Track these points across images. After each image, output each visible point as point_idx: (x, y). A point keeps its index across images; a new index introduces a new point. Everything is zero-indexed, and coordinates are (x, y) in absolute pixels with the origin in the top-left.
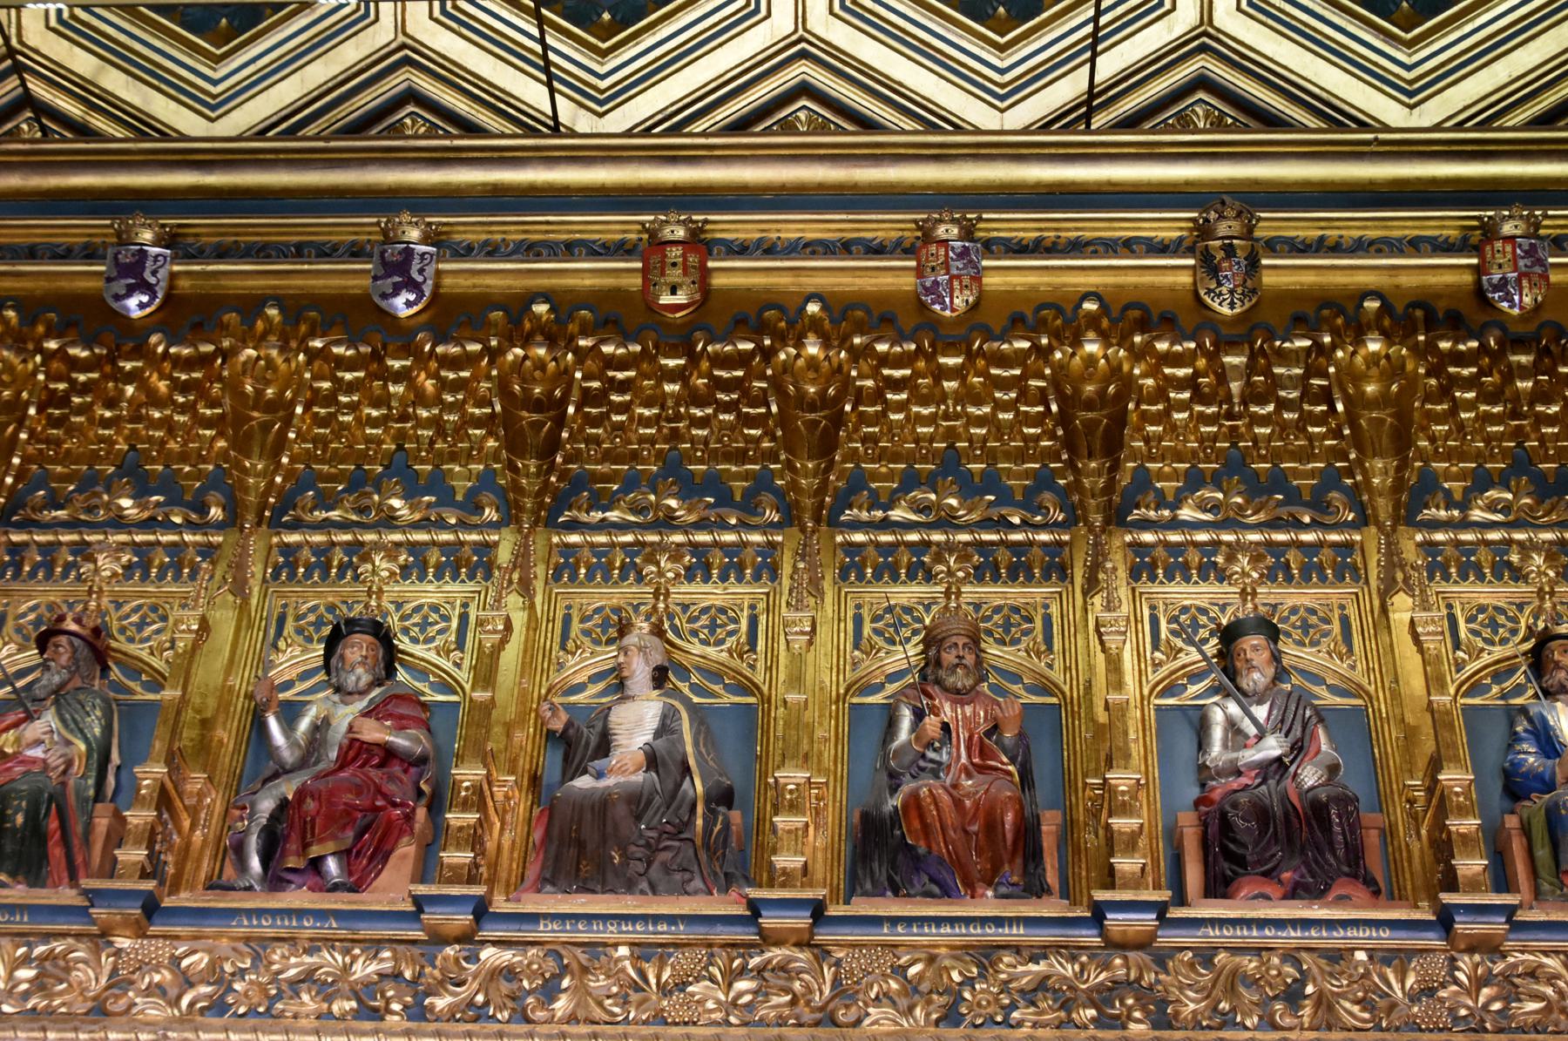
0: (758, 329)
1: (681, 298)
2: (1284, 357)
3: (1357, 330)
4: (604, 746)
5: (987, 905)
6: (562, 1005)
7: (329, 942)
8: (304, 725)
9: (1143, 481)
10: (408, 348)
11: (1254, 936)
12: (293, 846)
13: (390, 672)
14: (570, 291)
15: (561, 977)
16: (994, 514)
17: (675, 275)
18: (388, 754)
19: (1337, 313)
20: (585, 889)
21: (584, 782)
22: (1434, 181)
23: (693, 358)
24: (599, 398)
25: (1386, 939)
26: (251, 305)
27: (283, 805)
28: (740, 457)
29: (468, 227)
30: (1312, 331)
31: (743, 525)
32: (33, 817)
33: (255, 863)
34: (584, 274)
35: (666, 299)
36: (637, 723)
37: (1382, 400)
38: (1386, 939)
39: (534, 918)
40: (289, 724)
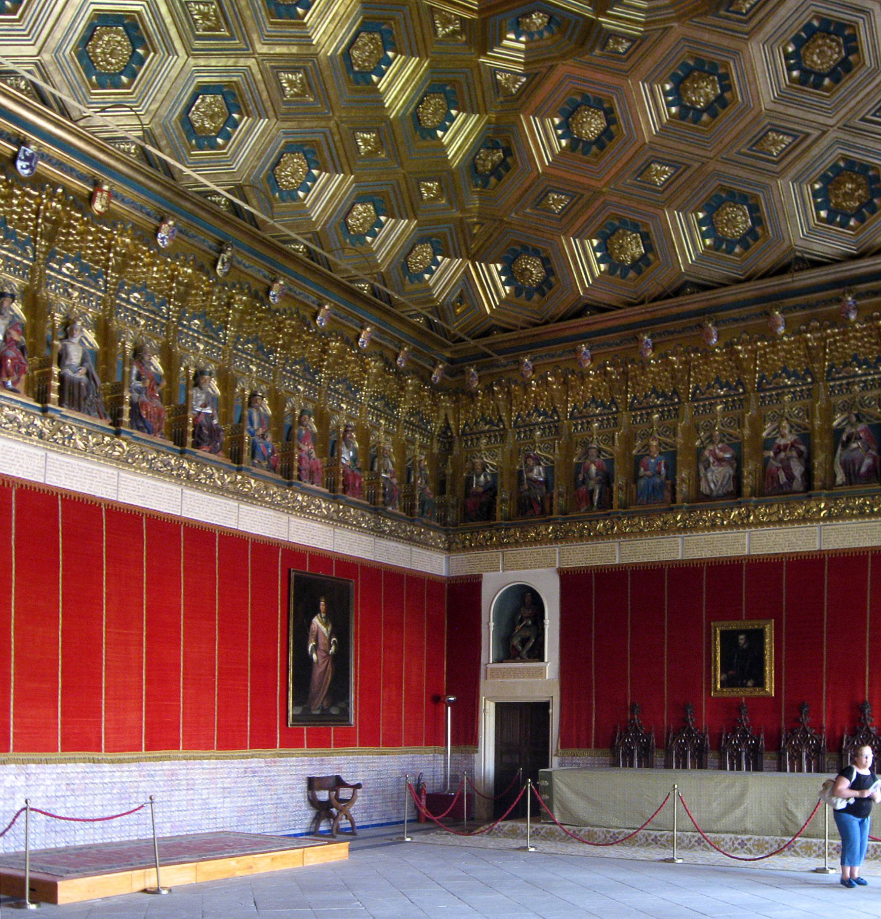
36: (75, 355)
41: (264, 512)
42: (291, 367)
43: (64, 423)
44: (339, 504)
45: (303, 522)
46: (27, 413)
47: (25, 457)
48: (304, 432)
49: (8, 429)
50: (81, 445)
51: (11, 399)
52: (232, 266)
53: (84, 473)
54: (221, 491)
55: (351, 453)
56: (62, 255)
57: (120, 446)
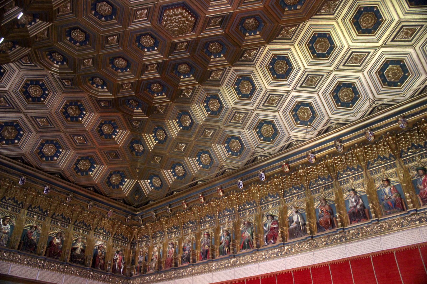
0: (296, 170)
2: (349, 154)
3: (355, 148)
4: (293, 221)
5: (328, 231)
6: (293, 251)
8: (267, 226)
9: (339, 173)
11: (354, 228)
13: (273, 218)
19: (353, 147)
21: (291, 227)
22: (360, 126)
23: (291, 176)
24: (284, 182)
25: (367, 225)
27: (267, 236)
28: (299, 184)
30: (351, 150)
31: (301, 191)
32: (248, 243)
34: (277, 170)
37: (361, 155)
38: (367, 225)
40: (266, 227)
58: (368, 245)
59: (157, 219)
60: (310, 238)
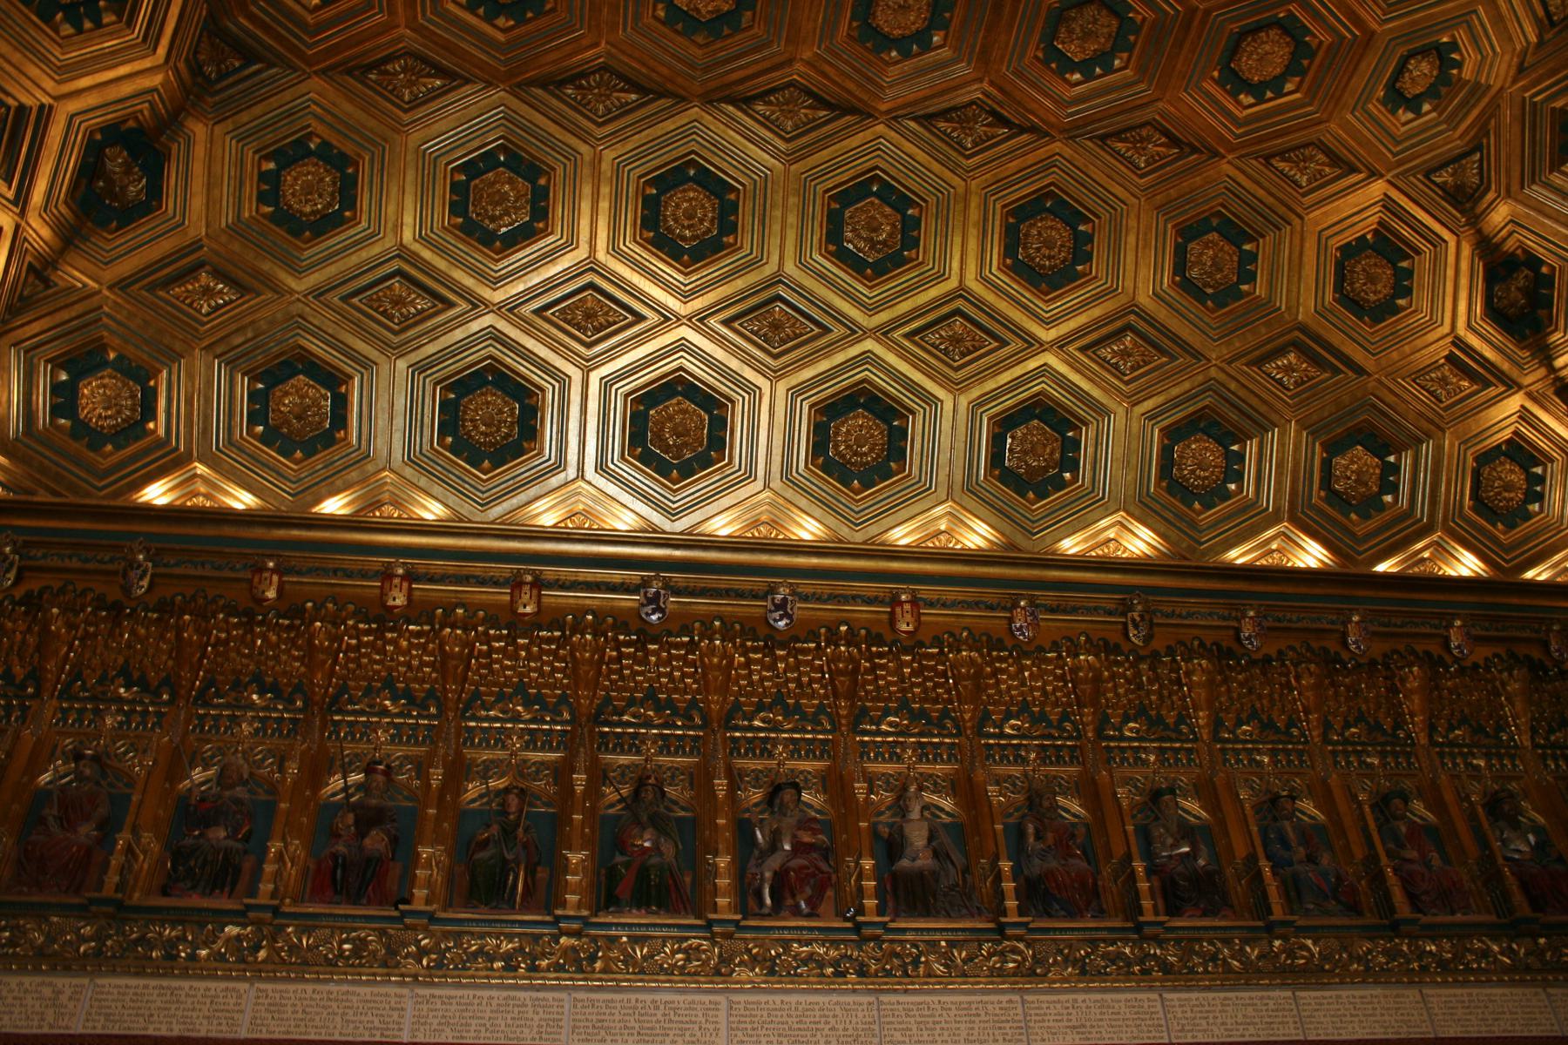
1: (911, 628)
7: (816, 940)
10: (783, 646)
12: (787, 895)
14: (857, 620)
15: (919, 957)
16: (1046, 732)
17: (908, 617)
18: (811, 847)
20: (921, 915)
21: (905, 863)
26: (706, 621)
27: (775, 873)
29: (807, 585)
33: (768, 901)
35: (904, 627)
36: (917, 836)
39: (904, 930)
41: (1357, 993)
42: (1342, 734)
43: (901, 942)
44: (1535, 936)
45: (1459, 991)
46: (833, 942)
47: (838, 1012)
48: (1404, 829)
49: (801, 975)
50: (939, 968)
51: (801, 928)
52: (1152, 625)
53: (952, 1013)
54: (1249, 976)
55: (1531, 838)
56: (878, 709)
57: (1014, 951)
58: (1250, 1009)
59: (18, 594)
60: (1009, 932)
